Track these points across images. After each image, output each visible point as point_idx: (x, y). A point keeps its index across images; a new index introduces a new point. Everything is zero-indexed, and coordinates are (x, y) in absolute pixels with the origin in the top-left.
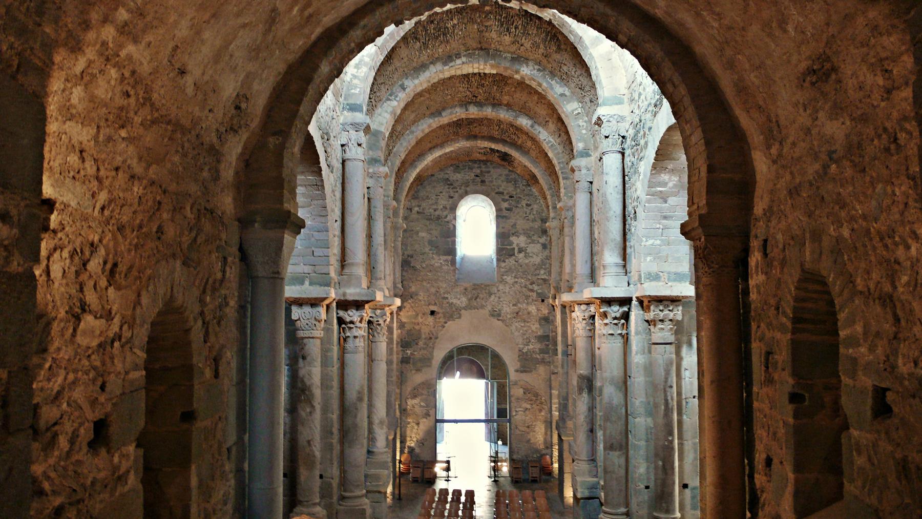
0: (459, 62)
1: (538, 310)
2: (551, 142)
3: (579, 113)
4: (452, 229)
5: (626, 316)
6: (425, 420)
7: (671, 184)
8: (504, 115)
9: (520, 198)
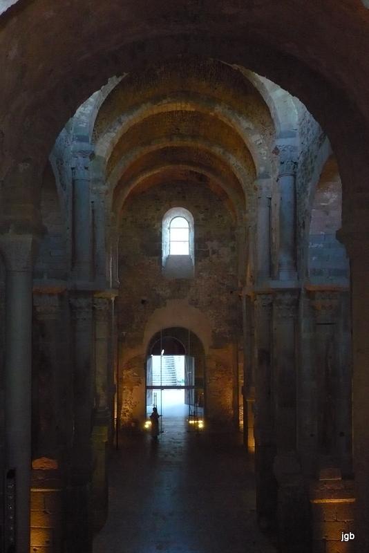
0: (165, 101)
2: (238, 166)
5: (296, 304)
6: (137, 387)
7: (331, 201)
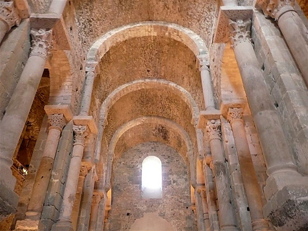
1: (185, 213)
2: (186, 92)
3: (199, 39)
4: (140, 171)
8: (162, 82)
9: (173, 158)
